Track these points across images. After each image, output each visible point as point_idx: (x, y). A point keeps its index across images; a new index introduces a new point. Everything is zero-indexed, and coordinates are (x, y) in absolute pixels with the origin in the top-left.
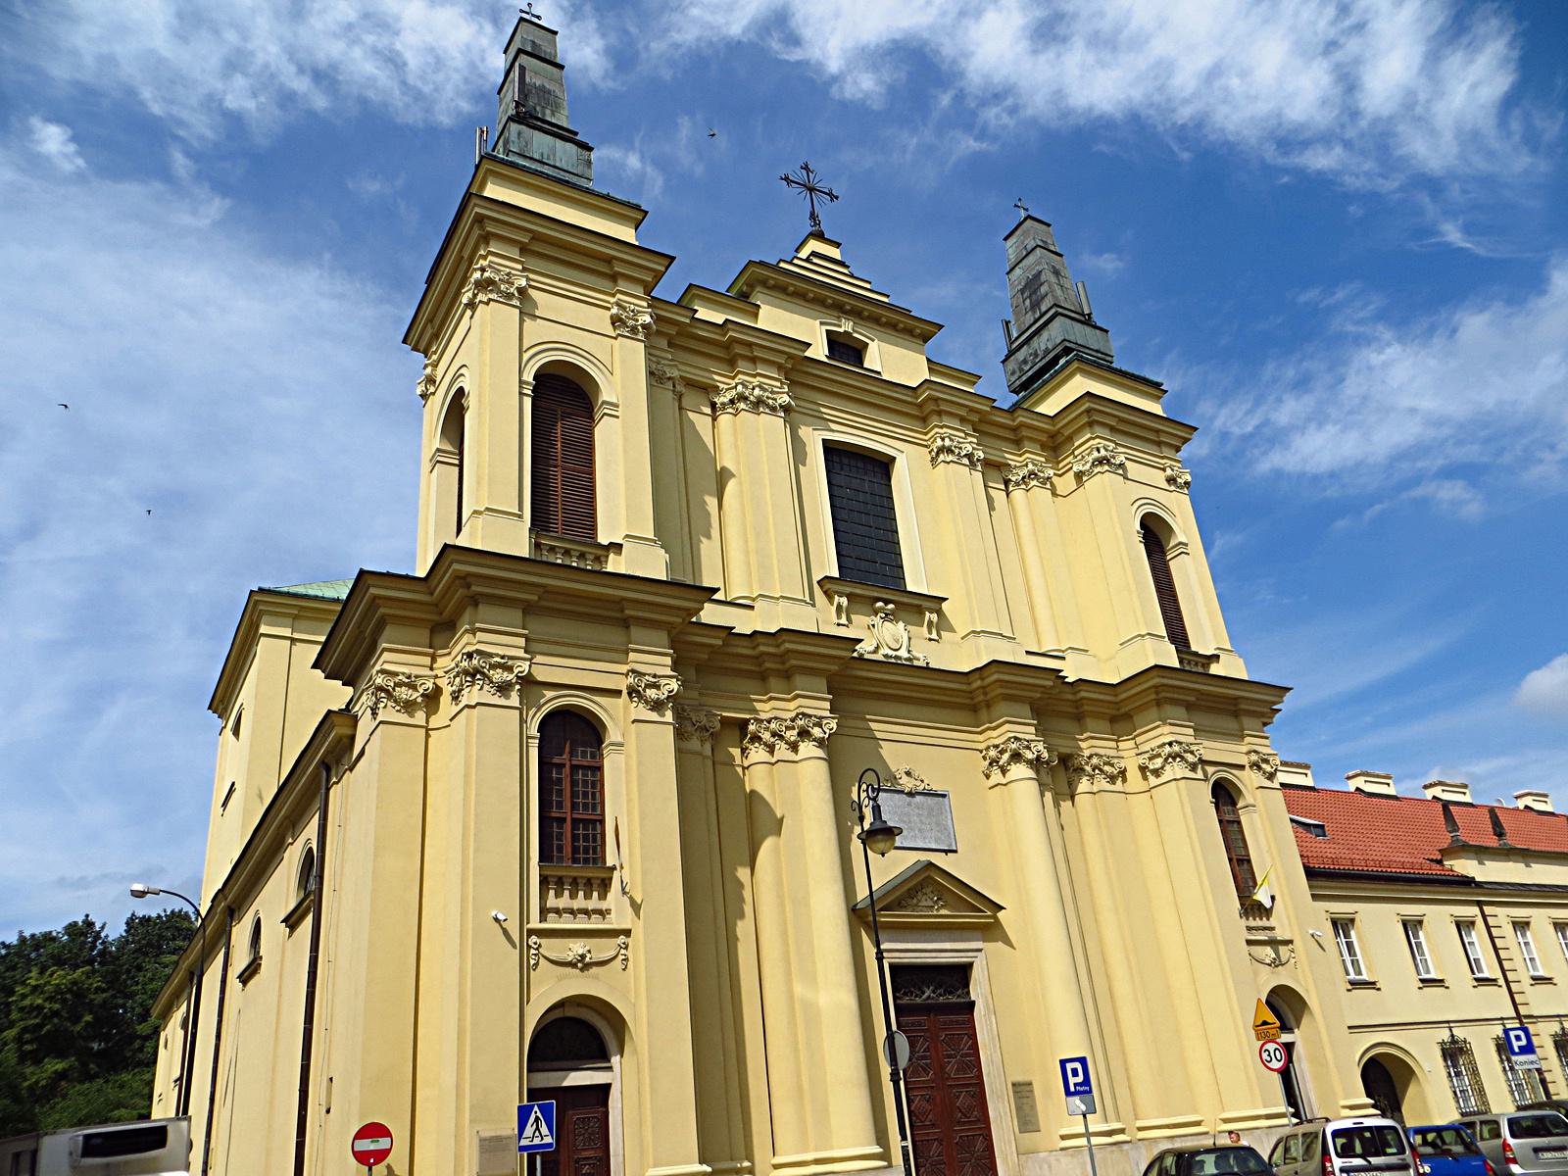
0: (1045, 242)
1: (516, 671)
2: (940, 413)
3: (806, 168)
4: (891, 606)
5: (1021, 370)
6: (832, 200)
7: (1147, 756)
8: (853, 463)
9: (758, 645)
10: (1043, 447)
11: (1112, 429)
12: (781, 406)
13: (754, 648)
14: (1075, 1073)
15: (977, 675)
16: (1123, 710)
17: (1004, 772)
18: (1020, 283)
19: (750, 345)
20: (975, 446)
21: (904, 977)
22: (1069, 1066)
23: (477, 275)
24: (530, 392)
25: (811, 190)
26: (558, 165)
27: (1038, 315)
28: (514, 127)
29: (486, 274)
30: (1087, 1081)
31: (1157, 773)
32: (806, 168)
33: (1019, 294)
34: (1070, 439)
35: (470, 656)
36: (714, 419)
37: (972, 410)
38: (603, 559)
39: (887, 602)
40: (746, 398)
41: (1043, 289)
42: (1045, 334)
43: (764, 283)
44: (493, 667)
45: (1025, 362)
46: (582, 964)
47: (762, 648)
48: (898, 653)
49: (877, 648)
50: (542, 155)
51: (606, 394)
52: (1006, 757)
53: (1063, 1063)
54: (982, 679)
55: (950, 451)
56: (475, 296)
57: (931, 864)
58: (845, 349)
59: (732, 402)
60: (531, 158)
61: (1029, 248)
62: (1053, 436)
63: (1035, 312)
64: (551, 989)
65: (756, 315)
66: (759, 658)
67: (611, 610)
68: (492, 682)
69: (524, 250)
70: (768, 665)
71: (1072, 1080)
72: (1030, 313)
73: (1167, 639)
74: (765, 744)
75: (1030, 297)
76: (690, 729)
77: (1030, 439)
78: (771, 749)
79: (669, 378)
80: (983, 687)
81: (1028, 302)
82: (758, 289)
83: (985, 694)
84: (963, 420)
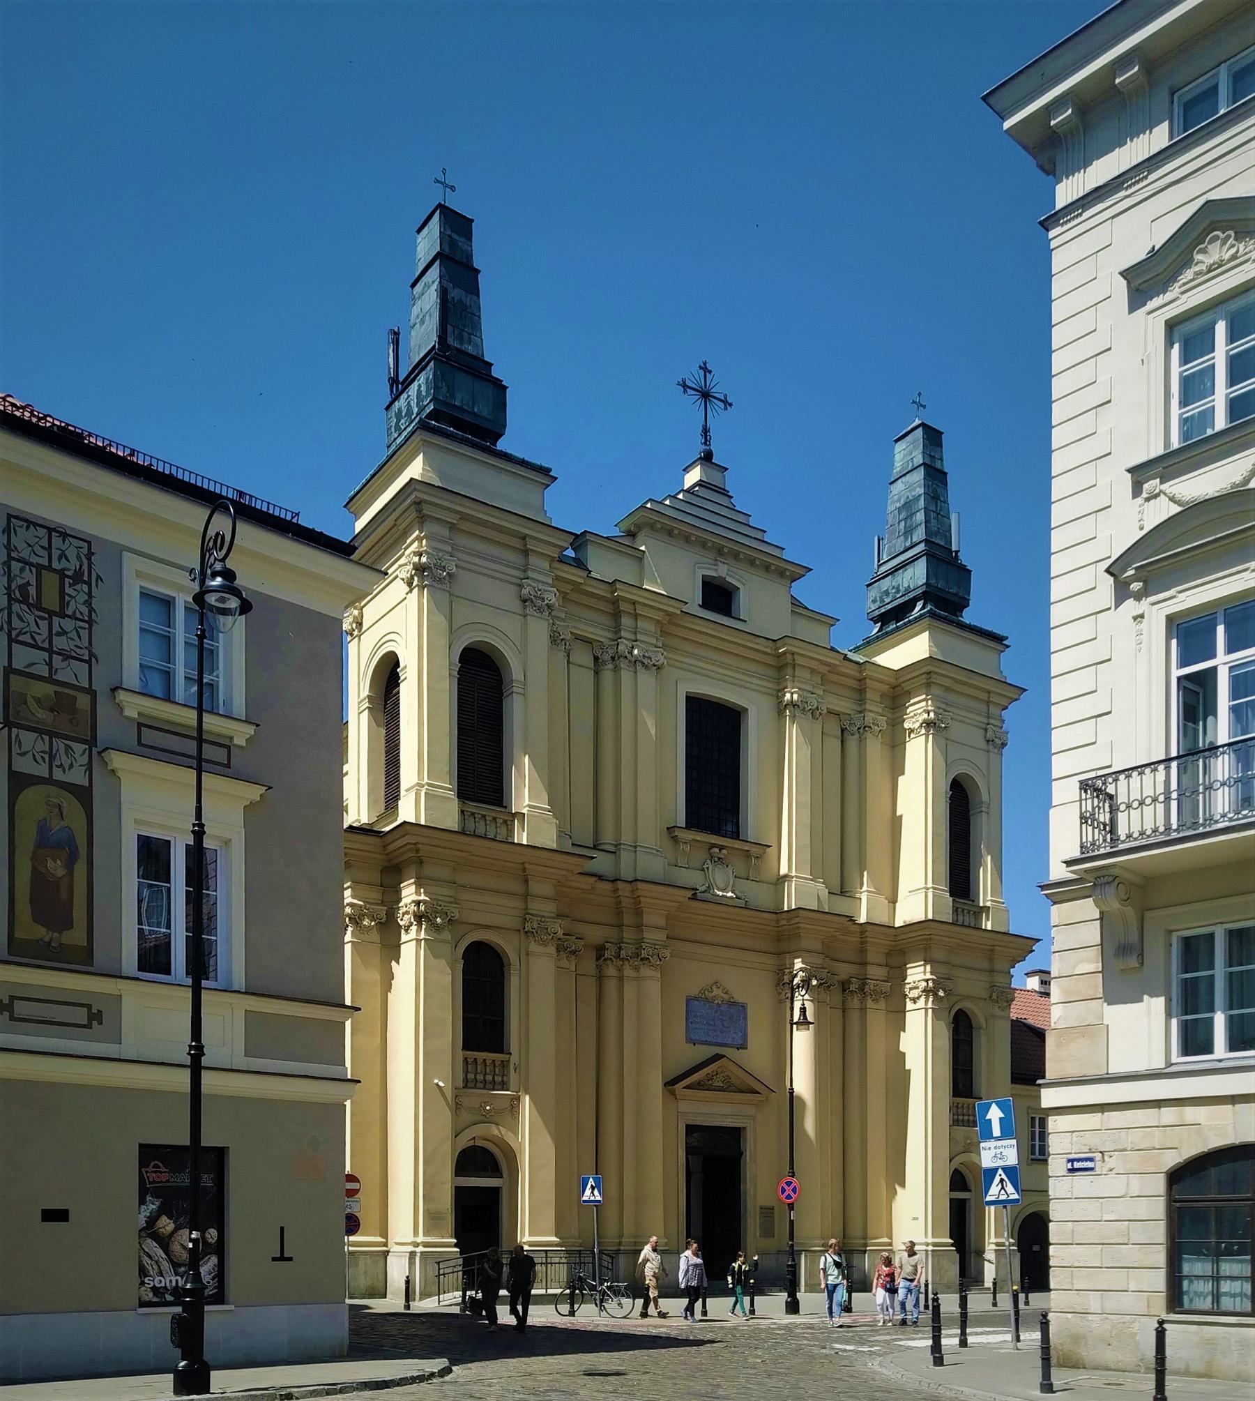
36: (596, 673)
64: (464, 1141)
78: (620, 969)
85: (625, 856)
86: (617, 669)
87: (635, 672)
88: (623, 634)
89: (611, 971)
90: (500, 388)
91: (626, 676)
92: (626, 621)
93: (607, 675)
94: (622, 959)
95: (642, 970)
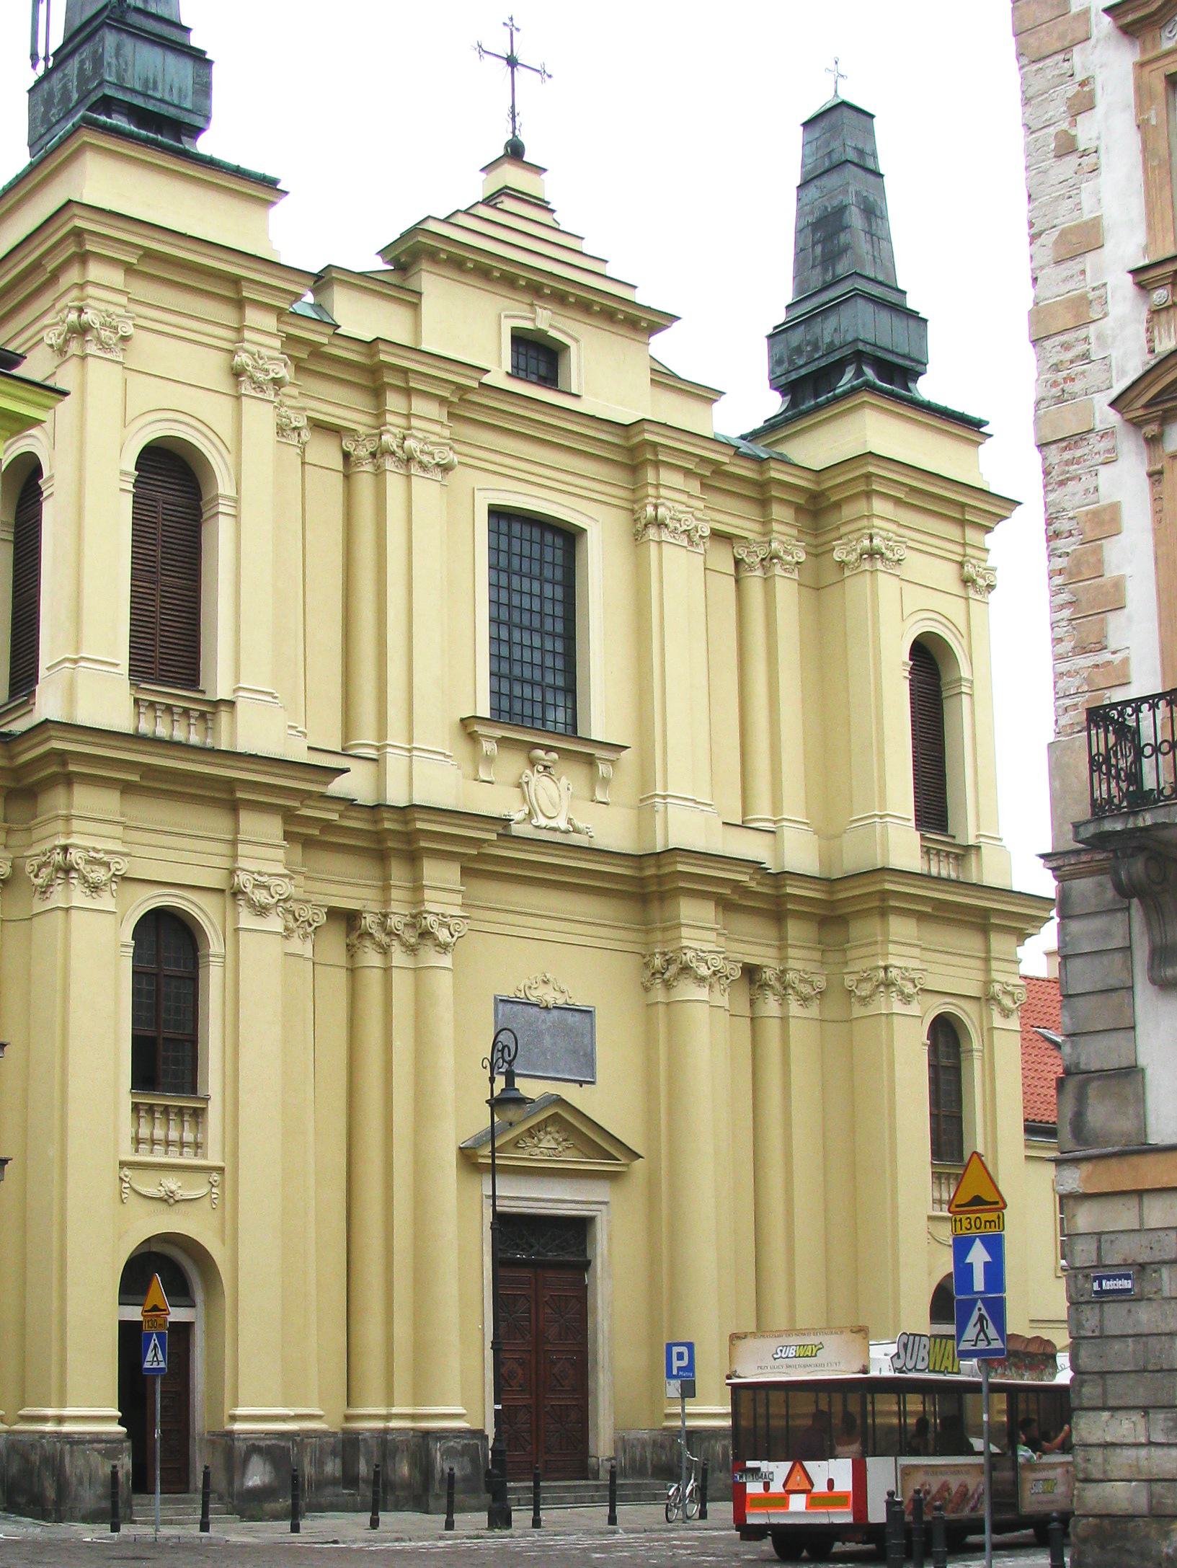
0: (861, 152)
1: (113, 869)
2: (657, 464)
3: (511, 26)
4: (554, 756)
5: (791, 362)
6: (543, 81)
7: (854, 977)
8: (526, 530)
9: (382, 820)
10: (798, 509)
11: (898, 502)
12: (438, 465)
13: (376, 822)
14: (680, 1356)
15: (652, 861)
16: (839, 912)
17: (668, 985)
18: (812, 213)
19: (405, 371)
20: (699, 515)
21: (511, 1230)
22: (676, 1350)
23: (73, 317)
24: (130, 487)
25: (512, 62)
26: (167, 98)
27: (829, 277)
28: (110, 39)
29: (84, 317)
30: (690, 1367)
31: (864, 1001)
32: (511, 26)
33: (808, 231)
34: (838, 505)
35: (65, 849)
36: (347, 477)
37: (703, 459)
38: (209, 716)
39: (549, 749)
40: (393, 453)
41: (844, 238)
42: (832, 322)
43: (433, 255)
44: (93, 862)
45: (798, 350)
46: (168, 1200)
47: (387, 825)
48: (552, 824)
49: (530, 815)
50: (147, 80)
51: (224, 486)
52: (673, 969)
53: (669, 1347)
54: (659, 867)
55: (660, 524)
56: (66, 341)
57: (560, 1101)
58: (539, 357)
59: (373, 455)
60: (132, 91)
61: (836, 158)
62: (815, 496)
63: (825, 270)
65: (415, 307)
66: (379, 836)
67: (220, 787)
68: (87, 881)
69: (129, 269)
70: (390, 844)
71: (676, 1364)
72: (818, 269)
73: (913, 823)
74: (380, 945)
75: (823, 242)
76: (292, 924)
77: (782, 501)
78: (385, 951)
79: (295, 429)
80: (657, 876)
81: (819, 249)
82: (425, 265)
83: (660, 884)
84: (688, 473)
85: (395, 762)
86: (379, 473)
87: (409, 477)
88: (389, 418)
89: (371, 957)
90: (199, 59)
91: (394, 483)
92: (393, 401)
93: (364, 483)
94: (389, 934)
95: (422, 952)
